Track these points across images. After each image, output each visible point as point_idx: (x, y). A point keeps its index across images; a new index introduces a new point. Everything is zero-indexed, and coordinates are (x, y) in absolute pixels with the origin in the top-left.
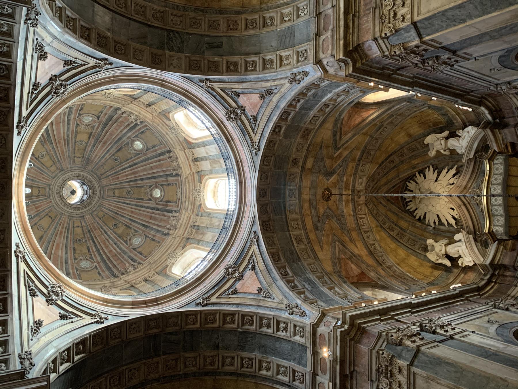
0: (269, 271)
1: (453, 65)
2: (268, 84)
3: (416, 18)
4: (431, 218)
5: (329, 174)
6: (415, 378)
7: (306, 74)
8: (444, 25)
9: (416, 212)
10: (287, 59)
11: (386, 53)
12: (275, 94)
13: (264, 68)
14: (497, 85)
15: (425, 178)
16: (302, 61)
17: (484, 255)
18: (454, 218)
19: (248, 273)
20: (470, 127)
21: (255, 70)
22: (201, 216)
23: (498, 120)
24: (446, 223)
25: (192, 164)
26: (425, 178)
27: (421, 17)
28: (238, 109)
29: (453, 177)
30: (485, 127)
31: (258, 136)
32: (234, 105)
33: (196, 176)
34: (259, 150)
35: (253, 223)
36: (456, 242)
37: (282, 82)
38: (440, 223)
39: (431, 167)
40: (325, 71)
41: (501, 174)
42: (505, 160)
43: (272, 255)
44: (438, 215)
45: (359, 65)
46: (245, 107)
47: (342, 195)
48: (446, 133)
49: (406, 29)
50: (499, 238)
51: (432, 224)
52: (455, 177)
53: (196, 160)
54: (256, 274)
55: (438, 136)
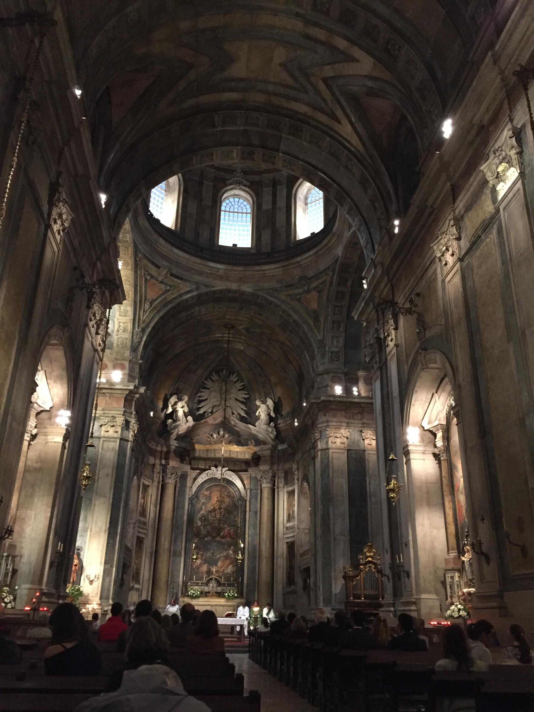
0: (166, 305)
1: (308, 452)
2: (322, 320)
3: (331, 451)
4: (204, 394)
5: (247, 329)
6: (113, 441)
7: (323, 356)
8: (323, 465)
9: (210, 380)
10: (337, 342)
11: (318, 426)
12: (314, 324)
13: (334, 322)
14: (298, 462)
15: (239, 390)
16: (332, 356)
17: (175, 439)
18: (205, 412)
19: (163, 286)
20: (275, 433)
21: (334, 314)
22: (214, 187)
23: (277, 452)
24: (200, 406)
25: (270, 176)
26: (239, 390)
27: (330, 453)
28: (308, 288)
29: (238, 414)
30: (273, 446)
31: (283, 298)
32: (313, 286)
33: (257, 178)
34: (271, 296)
35: (206, 286)
36: (186, 418)
37: (322, 333)
38: (200, 402)
39: (248, 396)
40: (319, 375)
41: (237, 456)
42: (247, 459)
43: (179, 304)
44: (206, 399)
45: (315, 405)
46: (309, 294)
47: (229, 334)
48: (273, 414)
49: (327, 443)
50: (191, 452)
51: (199, 394)
52: (238, 416)
53: (275, 184)
54: (163, 294)
55: (272, 409)
